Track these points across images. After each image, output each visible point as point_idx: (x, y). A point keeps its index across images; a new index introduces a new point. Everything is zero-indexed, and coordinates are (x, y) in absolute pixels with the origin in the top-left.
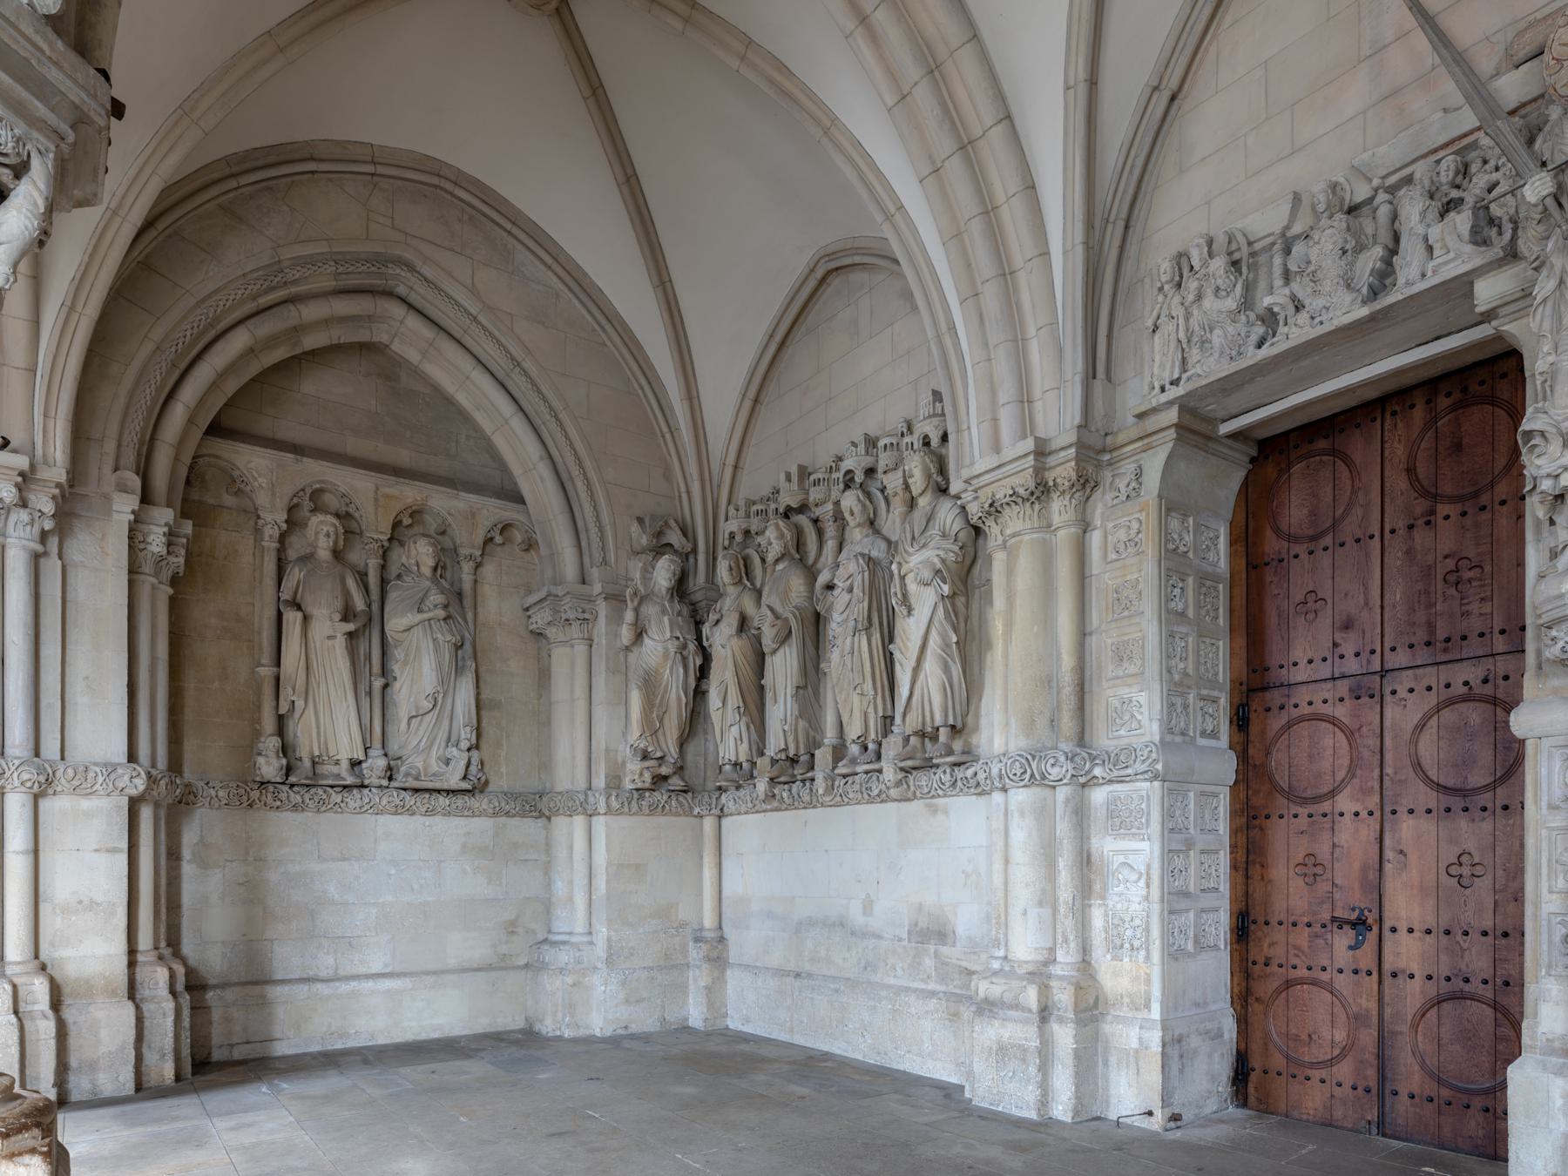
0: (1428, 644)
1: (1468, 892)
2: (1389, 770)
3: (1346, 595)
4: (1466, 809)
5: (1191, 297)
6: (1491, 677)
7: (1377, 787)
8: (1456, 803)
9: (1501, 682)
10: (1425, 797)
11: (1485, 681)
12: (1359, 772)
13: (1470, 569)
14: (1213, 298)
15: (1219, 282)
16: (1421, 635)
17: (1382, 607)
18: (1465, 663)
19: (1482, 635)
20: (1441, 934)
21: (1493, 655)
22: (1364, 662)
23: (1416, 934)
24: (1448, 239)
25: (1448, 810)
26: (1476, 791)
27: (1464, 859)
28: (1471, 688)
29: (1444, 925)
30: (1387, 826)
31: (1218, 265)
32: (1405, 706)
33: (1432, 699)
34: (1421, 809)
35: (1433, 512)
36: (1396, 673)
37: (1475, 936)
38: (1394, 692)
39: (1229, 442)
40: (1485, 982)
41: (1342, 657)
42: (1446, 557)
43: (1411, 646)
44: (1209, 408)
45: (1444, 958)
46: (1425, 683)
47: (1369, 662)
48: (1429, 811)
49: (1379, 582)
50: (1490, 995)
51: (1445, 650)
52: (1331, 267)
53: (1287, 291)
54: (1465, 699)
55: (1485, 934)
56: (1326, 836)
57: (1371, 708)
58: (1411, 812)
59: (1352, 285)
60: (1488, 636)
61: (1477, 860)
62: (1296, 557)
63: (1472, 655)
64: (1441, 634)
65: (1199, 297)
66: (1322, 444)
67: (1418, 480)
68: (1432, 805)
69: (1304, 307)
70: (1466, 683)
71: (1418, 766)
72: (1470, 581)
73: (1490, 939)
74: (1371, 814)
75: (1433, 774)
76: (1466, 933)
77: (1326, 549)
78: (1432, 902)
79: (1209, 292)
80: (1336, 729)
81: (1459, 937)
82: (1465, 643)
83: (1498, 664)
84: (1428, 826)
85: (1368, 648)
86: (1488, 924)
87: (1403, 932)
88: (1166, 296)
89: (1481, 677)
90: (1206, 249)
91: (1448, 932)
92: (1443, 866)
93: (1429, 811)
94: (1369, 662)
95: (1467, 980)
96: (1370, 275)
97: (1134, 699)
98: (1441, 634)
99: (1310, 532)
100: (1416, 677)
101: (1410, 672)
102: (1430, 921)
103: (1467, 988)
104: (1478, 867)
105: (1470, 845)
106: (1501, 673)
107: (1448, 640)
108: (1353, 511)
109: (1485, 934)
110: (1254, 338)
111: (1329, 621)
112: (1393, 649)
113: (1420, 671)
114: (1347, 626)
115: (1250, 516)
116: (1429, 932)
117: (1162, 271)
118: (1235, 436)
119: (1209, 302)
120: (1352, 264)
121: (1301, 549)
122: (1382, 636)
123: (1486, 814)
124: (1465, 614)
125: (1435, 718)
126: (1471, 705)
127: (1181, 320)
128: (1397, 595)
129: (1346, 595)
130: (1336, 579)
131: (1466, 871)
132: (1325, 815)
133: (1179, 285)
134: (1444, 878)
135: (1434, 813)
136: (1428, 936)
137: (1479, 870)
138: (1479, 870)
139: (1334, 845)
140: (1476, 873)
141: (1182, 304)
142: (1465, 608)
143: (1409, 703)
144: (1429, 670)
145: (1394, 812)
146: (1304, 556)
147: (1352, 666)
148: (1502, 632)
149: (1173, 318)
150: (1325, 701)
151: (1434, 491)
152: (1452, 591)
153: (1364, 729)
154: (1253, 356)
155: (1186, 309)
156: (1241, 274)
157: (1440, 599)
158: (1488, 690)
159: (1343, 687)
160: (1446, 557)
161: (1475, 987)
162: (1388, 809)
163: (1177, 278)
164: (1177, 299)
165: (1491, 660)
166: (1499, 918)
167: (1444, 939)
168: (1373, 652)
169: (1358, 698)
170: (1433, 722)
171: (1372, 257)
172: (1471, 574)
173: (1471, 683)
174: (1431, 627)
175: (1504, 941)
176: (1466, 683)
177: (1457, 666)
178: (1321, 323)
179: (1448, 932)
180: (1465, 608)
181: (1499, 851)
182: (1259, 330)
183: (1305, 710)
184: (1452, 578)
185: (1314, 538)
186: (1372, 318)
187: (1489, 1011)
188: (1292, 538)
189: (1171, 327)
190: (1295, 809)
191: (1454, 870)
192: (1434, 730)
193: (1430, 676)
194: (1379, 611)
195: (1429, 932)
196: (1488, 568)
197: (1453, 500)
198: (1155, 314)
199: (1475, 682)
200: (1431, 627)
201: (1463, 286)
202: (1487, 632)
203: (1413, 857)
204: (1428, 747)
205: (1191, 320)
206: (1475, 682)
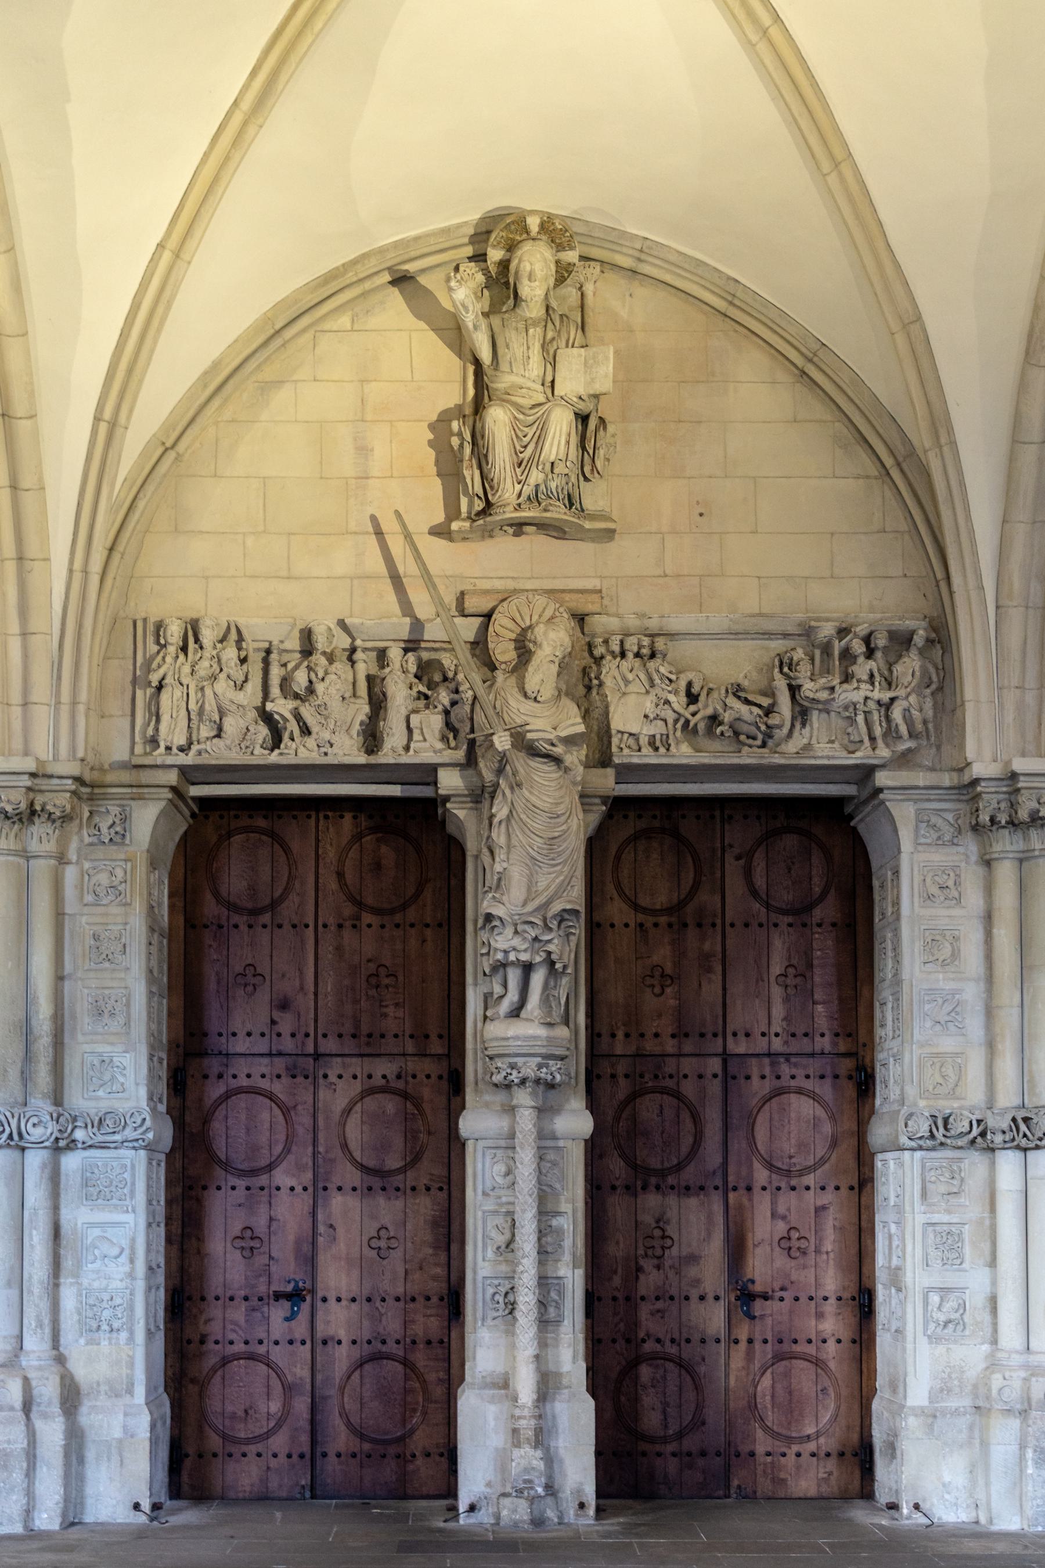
0: (354, 1036)
1: (385, 1262)
2: (321, 1149)
3: (283, 976)
4: (384, 1189)
6: (403, 1074)
7: (310, 1164)
8: (376, 1182)
9: (410, 1079)
10: (351, 1176)
11: (399, 1077)
12: (294, 1148)
13: (387, 976)
16: (348, 1028)
17: (316, 994)
18: (383, 1059)
19: (396, 1036)
20: (364, 1301)
21: (404, 1055)
22: (300, 1045)
23: (344, 1303)
25: (370, 1189)
26: (391, 1173)
27: (383, 1233)
28: (388, 1081)
29: (366, 1293)
30: (320, 1202)
32: (335, 1090)
33: (357, 1087)
34: (347, 1187)
35: (358, 918)
36: (327, 1059)
37: (390, 1301)
38: (325, 1076)
40: (398, 1342)
41: (279, 1035)
42: (369, 961)
43: (340, 1036)
45: (366, 1323)
46: (351, 1071)
47: (303, 1043)
48: (354, 1189)
49: (312, 970)
50: (401, 1353)
51: (368, 1044)
54: (384, 1090)
55: (398, 1299)
56: (263, 1209)
57: (306, 1088)
58: (340, 1189)
60: (401, 1038)
61: (392, 1234)
62: (236, 926)
63: (388, 1052)
64: (365, 1030)
67: (346, 884)
68: (357, 1184)
70: (384, 1077)
71: (345, 1146)
72: (387, 986)
73: (401, 1304)
74: (305, 1189)
75: (357, 1155)
76: (383, 1300)
77: (264, 926)
78: (356, 1273)
80: (273, 1105)
81: (378, 1304)
82: (383, 1040)
83: (409, 1064)
84: (353, 1202)
85: (303, 1031)
86: (400, 1290)
87: (332, 1301)
89: (395, 1073)
91: (369, 1300)
92: (365, 1239)
93: (354, 1189)
94: (303, 1043)
95: (384, 1342)
97: (115, 1059)
98: (365, 1030)
99: (250, 905)
100: (344, 1064)
101: (339, 1060)
102: (355, 1290)
103: (384, 1349)
104: (393, 1241)
105: (386, 1221)
106: (410, 1072)
107: (370, 1036)
108: (290, 897)
109: (398, 1299)
111: (267, 998)
112: (325, 1036)
113: (348, 1060)
114: (284, 1005)
115: (189, 872)
116: (354, 1300)
121: (241, 920)
122: (316, 1021)
123: (399, 1193)
124: (385, 1015)
125: (359, 1105)
126: (388, 1096)
128: (328, 985)
129: (283, 976)
130: (274, 958)
131: (383, 1244)
132: (262, 1189)
134: (366, 1250)
135: (359, 1191)
136: (353, 1304)
137: (394, 1243)
138: (394, 1243)
139: (271, 1219)
140: (392, 1246)
142: (385, 1010)
143: (339, 1088)
144: (354, 1060)
145: (325, 1189)
146: (243, 928)
147: (288, 1045)
148: (412, 1036)
150: (263, 1076)
152: (373, 992)
153: (300, 1107)
157: (364, 998)
158: (400, 1085)
159: (280, 1064)
160: (369, 961)
161: (391, 1347)
162: (321, 1185)
165: (402, 1058)
166: (409, 1285)
167: (366, 1306)
168: (307, 1035)
169: (294, 1077)
170: (358, 1107)
172: (386, 981)
173: (389, 1077)
174: (357, 1023)
175: (412, 1305)
176: (384, 1077)
177: (377, 1059)
179: (369, 1300)
180: (385, 1010)
181: (409, 1226)
183: (244, 1082)
184: (373, 981)
185: (255, 912)
187: (400, 1368)
188: (233, 907)
190: (233, 1181)
191: (374, 1243)
192: (359, 1115)
193: (356, 1065)
194: (312, 997)
195: (354, 1300)
196: (401, 978)
197: (377, 911)
199: (391, 1077)
200: (357, 1023)
202: (400, 1034)
203: (341, 1231)
204: (354, 1131)
206: (391, 1077)
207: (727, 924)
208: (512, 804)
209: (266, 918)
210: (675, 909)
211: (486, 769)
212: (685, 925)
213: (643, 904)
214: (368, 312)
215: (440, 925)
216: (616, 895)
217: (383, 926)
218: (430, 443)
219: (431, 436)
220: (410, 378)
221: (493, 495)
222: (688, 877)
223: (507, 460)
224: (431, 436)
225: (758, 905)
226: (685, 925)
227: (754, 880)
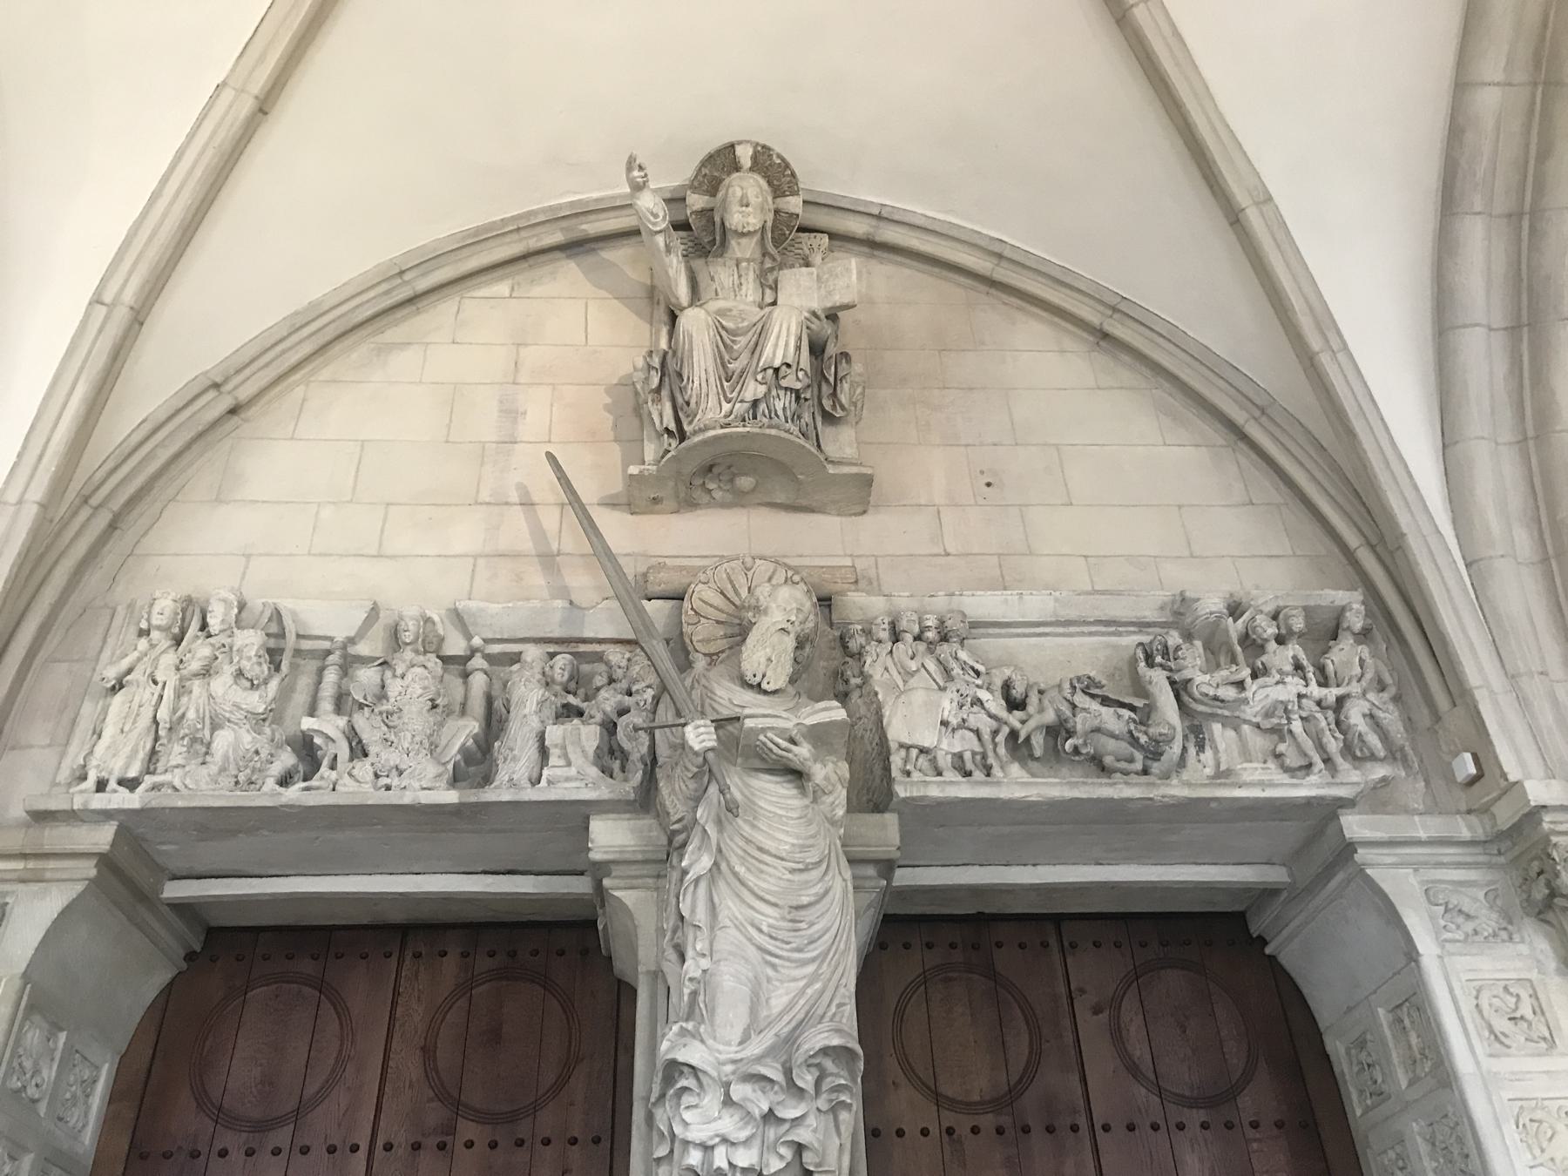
5: (195, 666)
14: (230, 680)
15: (246, 665)
24: (570, 749)
31: (251, 641)
39: (171, 916)
44: (164, 848)
52: (416, 720)
53: (342, 722)
59: (435, 755)
65: (206, 672)
66: (307, 966)
69: (366, 755)
79: (229, 670)
88: (152, 646)
90: (236, 610)
96: (459, 752)
110: (277, 769)
117: (156, 609)
118: (185, 909)
119: (222, 684)
120: (441, 724)
127: (169, 693)
133: (178, 641)
141: (178, 669)
149: (155, 683)
151: (455, 1094)
154: (269, 794)
155: (181, 680)
156: (278, 669)
163: (176, 630)
164: (170, 658)
171: (465, 730)
178: (388, 788)
182: (287, 759)
186: (457, 811)
189: (148, 694)
198: (125, 664)
201: (575, 817)
205: (184, 699)
207: (1098, 1127)
208: (720, 850)
209: (282, 1137)
210: (1006, 1100)
211: (672, 794)
212: (1026, 1130)
213: (950, 1094)
214: (532, 281)
215: (597, 1141)
216: (901, 1078)
217: (493, 1145)
218: (607, 408)
219: (608, 400)
220: (584, 343)
221: (690, 423)
222: (1020, 1047)
223: (711, 370)
224: (608, 400)
225: (1143, 1091)
226: (1026, 1130)
227: (1129, 1048)
